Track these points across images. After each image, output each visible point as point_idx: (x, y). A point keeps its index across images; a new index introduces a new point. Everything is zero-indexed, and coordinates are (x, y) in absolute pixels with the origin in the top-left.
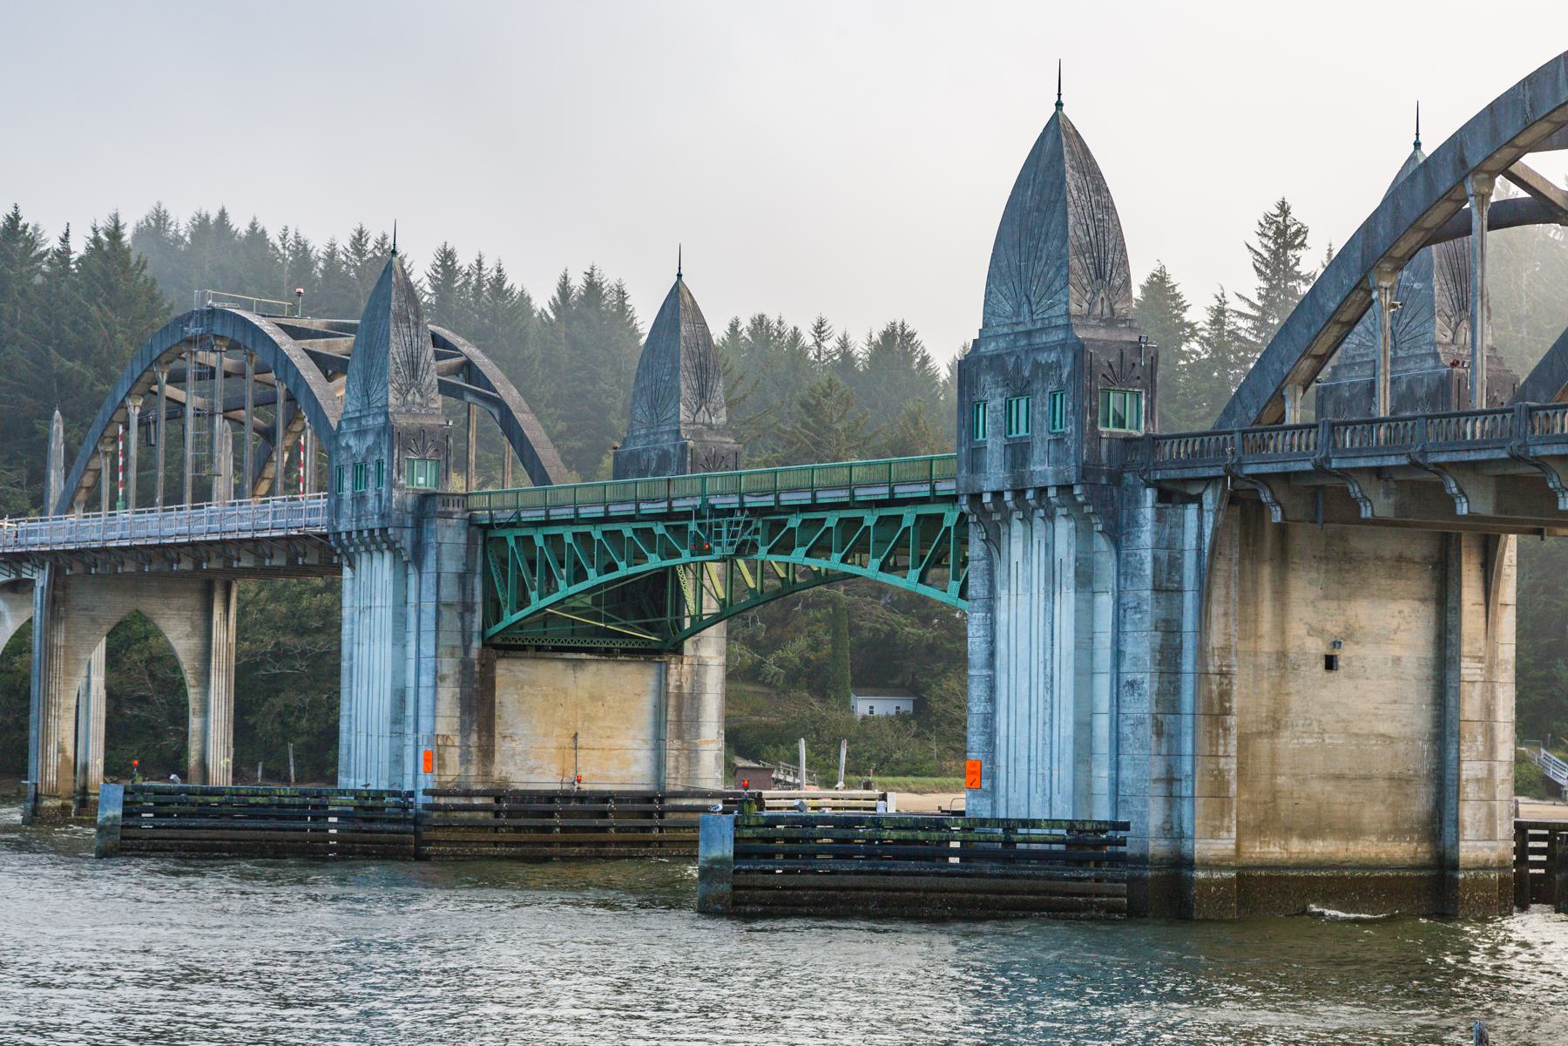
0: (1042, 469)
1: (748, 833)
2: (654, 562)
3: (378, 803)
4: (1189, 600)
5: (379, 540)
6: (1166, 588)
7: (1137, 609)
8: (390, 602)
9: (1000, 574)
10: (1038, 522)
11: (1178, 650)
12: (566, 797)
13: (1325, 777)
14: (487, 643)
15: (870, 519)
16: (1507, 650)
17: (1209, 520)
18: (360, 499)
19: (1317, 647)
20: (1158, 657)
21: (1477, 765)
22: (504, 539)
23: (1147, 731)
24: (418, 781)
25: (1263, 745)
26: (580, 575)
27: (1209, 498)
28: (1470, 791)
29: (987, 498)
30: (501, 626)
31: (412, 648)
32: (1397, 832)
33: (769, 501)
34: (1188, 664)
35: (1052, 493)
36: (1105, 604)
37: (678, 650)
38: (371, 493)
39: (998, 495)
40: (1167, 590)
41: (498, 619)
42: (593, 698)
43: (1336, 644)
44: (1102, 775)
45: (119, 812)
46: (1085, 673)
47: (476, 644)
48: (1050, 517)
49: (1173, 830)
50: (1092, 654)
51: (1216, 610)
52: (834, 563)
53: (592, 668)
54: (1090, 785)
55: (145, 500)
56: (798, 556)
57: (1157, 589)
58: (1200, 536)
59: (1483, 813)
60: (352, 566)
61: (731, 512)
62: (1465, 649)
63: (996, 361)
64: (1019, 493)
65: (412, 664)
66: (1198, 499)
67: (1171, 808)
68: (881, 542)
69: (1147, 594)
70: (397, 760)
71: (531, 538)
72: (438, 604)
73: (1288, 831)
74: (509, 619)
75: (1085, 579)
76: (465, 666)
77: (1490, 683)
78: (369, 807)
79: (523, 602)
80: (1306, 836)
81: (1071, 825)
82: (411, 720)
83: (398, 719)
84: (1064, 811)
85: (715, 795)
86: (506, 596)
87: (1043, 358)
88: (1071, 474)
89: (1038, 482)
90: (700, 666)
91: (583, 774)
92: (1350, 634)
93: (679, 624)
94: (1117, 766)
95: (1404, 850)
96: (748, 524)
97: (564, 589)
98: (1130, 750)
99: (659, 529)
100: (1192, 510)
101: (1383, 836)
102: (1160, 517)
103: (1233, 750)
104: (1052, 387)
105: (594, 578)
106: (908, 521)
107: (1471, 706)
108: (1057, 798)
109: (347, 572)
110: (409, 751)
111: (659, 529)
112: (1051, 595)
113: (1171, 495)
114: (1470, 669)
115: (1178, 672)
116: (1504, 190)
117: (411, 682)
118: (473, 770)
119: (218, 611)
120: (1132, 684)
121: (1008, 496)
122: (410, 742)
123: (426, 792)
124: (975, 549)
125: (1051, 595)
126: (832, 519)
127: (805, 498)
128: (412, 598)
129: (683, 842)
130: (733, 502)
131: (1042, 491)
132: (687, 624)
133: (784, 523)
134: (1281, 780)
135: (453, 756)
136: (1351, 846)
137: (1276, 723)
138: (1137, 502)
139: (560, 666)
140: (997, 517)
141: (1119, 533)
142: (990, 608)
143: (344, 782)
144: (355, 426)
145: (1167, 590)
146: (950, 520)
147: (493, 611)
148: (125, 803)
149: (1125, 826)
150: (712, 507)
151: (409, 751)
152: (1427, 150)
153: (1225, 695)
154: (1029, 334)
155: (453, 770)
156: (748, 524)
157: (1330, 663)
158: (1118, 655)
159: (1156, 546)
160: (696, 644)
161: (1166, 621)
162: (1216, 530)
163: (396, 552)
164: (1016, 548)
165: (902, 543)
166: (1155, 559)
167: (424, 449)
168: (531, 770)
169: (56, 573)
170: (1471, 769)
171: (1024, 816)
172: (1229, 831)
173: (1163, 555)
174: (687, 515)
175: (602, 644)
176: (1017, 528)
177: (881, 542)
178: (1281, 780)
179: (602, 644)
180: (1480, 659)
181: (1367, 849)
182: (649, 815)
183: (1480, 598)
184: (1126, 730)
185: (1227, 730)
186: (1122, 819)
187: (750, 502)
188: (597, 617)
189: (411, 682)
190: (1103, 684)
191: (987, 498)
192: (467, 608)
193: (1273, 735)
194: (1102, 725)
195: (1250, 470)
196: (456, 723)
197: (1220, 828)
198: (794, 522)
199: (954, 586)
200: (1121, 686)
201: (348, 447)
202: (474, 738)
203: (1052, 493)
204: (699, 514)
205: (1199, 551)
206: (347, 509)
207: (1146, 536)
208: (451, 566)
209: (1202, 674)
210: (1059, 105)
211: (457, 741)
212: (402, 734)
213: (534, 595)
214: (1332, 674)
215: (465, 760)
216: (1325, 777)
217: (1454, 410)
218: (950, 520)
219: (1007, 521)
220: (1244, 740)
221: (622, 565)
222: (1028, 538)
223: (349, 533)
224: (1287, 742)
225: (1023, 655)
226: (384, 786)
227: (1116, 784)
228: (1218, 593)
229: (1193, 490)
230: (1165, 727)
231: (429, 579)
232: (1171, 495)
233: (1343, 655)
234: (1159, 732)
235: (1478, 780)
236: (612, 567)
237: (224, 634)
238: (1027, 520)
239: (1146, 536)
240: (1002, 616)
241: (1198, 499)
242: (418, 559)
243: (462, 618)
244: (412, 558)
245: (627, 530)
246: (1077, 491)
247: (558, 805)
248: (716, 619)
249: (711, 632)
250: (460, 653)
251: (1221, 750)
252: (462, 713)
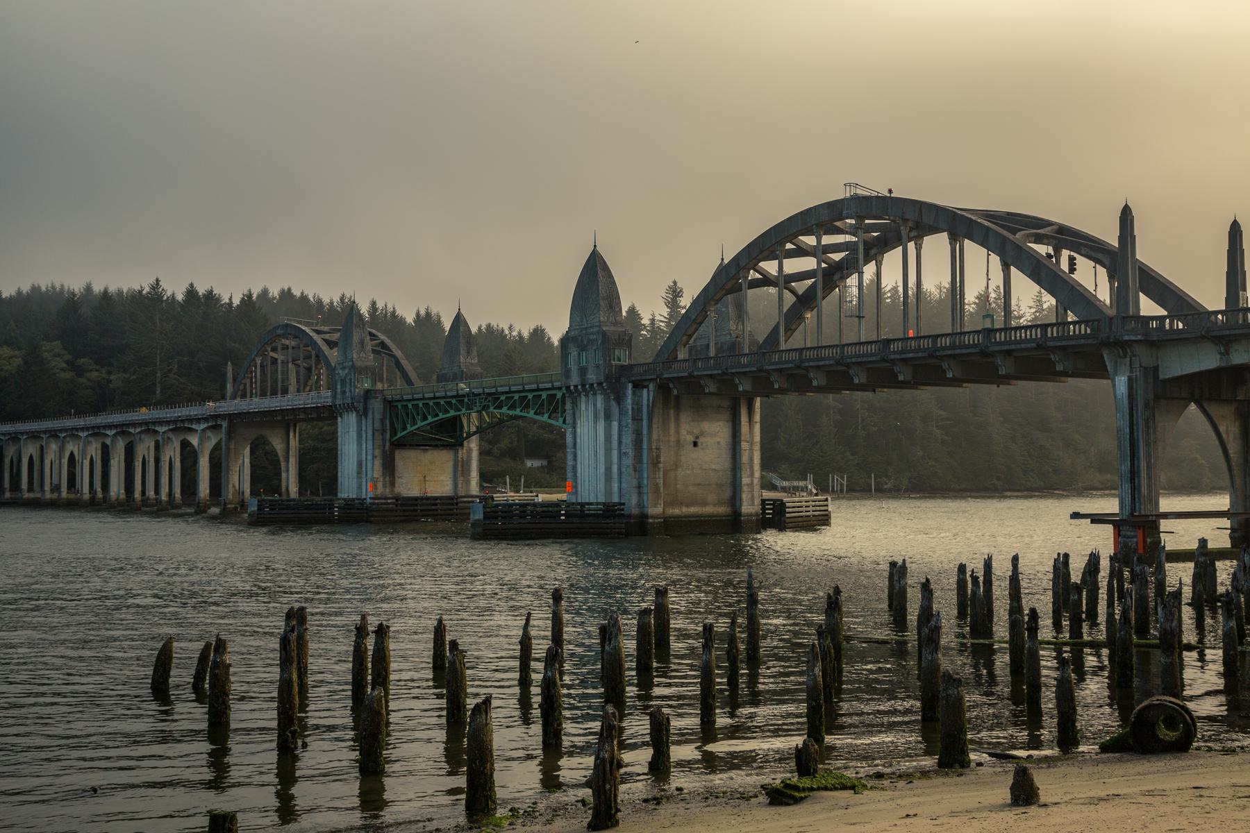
0: (592, 377)
1: (488, 510)
2: (452, 413)
3: (352, 503)
4: (645, 423)
5: (350, 407)
6: (637, 418)
7: (626, 426)
8: (355, 429)
9: (577, 415)
10: (590, 395)
11: (641, 441)
12: (422, 498)
13: (694, 485)
14: (392, 444)
15: (530, 396)
16: (757, 438)
17: (651, 394)
18: (344, 392)
19: (690, 438)
22: (397, 406)
23: (631, 470)
24: (368, 493)
25: (672, 474)
26: (425, 418)
27: (651, 387)
28: (745, 488)
29: (572, 388)
30: (397, 437)
31: (364, 446)
32: (720, 504)
33: (493, 390)
34: (645, 446)
35: (595, 385)
36: (615, 424)
37: (462, 445)
38: (347, 390)
39: (576, 387)
41: (396, 435)
42: (431, 463)
43: (697, 437)
44: (615, 486)
45: (256, 508)
46: (608, 450)
47: (388, 444)
48: (595, 394)
49: (640, 505)
50: (611, 443)
51: (654, 426)
52: (517, 412)
53: (430, 452)
54: (611, 489)
55: (263, 394)
56: (504, 410)
57: (634, 419)
58: (648, 400)
59: (749, 496)
60: (341, 417)
61: (480, 394)
62: (743, 438)
63: (574, 339)
64: (583, 386)
65: (364, 452)
66: (647, 387)
67: (640, 496)
68: (535, 404)
69: (630, 421)
70: (359, 487)
71: (407, 405)
72: (373, 429)
73: (681, 504)
74: (399, 435)
75: (608, 417)
76: (384, 452)
77: (751, 450)
78: (349, 504)
79: (404, 428)
80: (688, 506)
81: (604, 504)
82: (364, 472)
83: (359, 472)
84: (602, 499)
85: (477, 497)
86: (399, 426)
87: (592, 337)
88: (602, 378)
89: (590, 382)
90: (470, 450)
91: (428, 490)
92: (702, 434)
93: (462, 435)
94: (620, 482)
95: (722, 510)
96: (486, 399)
97: (420, 424)
98: (625, 477)
99: (454, 401)
100: (645, 391)
101: (715, 505)
102: (634, 393)
103: (661, 476)
104: (595, 348)
105: (430, 419)
106: (544, 397)
107: (745, 458)
108: (599, 495)
109: (339, 419)
110: (364, 483)
111: (454, 401)
112: (595, 422)
113: (638, 386)
114: (744, 445)
115: (641, 449)
116: (753, 275)
117: (364, 459)
118: (388, 490)
119: (291, 434)
120: (625, 453)
121: (579, 387)
122: (364, 480)
123: (370, 498)
124: (568, 406)
125: (595, 422)
126: (516, 397)
127: (507, 389)
128: (364, 428)
129: (465, 514)
130: (481, 391)
131: (592, 385)
132: (465, 435)
133: (499, 398)
134: (678, 486)
135: (380, 485)
137: (676, 466)
138: (626, 388)
139: (419, 451)
140: (576, 395)
141: (619, 399)
142: (574, 428)
143: (341, 495)
144: (341, 366)
146: (559, 396)
147: (394, 432)
148: (258, 505)
149: (624, 504)
150: (473, 393)
151: (364, 483)
152: (726, 261)
153: (658, 456)
154: (586, 328)
155: (380, 490)
156: (486, 399)
157: (695, 444)
158: (620, 443)
159: (633, 404)
160: (468, 442)
161: (637, 430)
162: (654, 397)
163: (358, 412)
164: (583, 406)
165: (542, 404)
166: (633, 409)
167: (367, 374)
168: (409, 490)
169: (230, 422)
170: (745, 480)
171: (587, 501)
173: (635, 407)
174: (464, 396)
175: (434, 443)
176: (583, 398)
177: (535, 404)
178: (678, 486)
179: (434, 443)
180: (748, 442)
181: (709, 510)
182: (452, 504)
183: (747, 420)
184: (623, 470)
185: (659, 469)
186: (623, 501)
187: (487, 391)
188: (432, 433)
189: (364, 459)
190: (615, 453)
191: (572, 388)
192: (384, 432)
193: (675, 470)
194: (615, 468)
195: (666, 376)
196: (381, 473)
198: (503, 398)
199: (561, 420)
200: (621, 454)
201: (339, 374)
202: (387, 479)
203: (595, 385)
204: (468, 395)
205: (648, 405)
206: (339, 396)
207: (629, 400)
208: (378, 416)
209: (650, 449)
210: (595, 246)
211: (381, 479)
212: (361, 478)
213: (408, 426)
215: (384, 486)
216: (694, 485)
217: (737, 353)
218: (559, 396)
219: (579, 395)
220: (665, 472)
221: (441, 414)
222: (587, 403)
223: (340, 405)
224: (680, 473)
225: (586, 444)
226: (355, 496)
227: (620, 489)
228: (655, 420)
229: (646, 384)
231: (370, 421)
232: (638, 386)
233: (700, 441)
234: (635, 470)
235: (748, 485)
236: (437, 415)
237: (294, 443)
238: (587, 395)
239: (629, 400)
240: (578, 430)
241: (647, 387)
242: (365, 414)
243: (382, 434)
244: (363, 414)
245: (442, 402)
246: (604, 385)
247: (419, 502)
248: (475, 433)
249: (474, 438)
250: (382, 448)
252: (383, 469)
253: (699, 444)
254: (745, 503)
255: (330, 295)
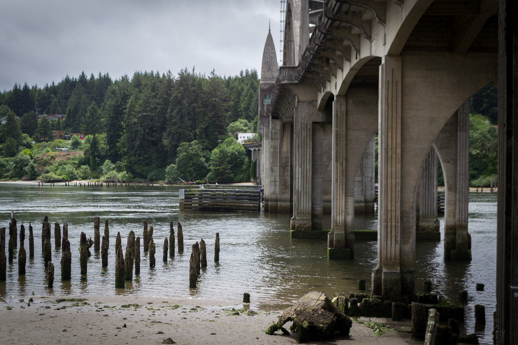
20: (272, 154)
21: (358, 178)
40: (274, 139)
51: (285, 143)
102: (272, 123)
145: (274, 139)
172: (288, 193)
173: (273, 131)
185: (287, 170)
197: (286, 192)
230: (274, 170)
235: (359, 181)
251: (286, 175)
255: (58, 80)
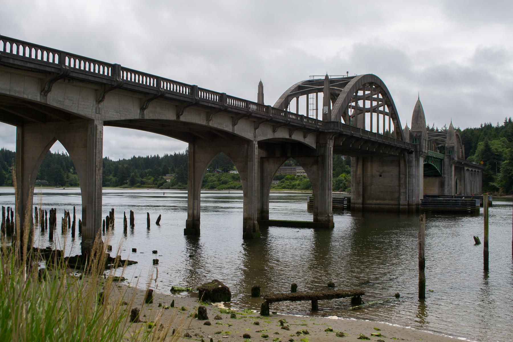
19: (378, 173)
32: (392, 200)
80: (376, 200)
134: (372, 192)
136: (384, 202)
170: (402, 190)
178: (372, 192)
180: (404, 175)
181: (386, 202)
214: (380, 177)
235: (403, 192)
253: (382, 176)
254: (402, 200)
